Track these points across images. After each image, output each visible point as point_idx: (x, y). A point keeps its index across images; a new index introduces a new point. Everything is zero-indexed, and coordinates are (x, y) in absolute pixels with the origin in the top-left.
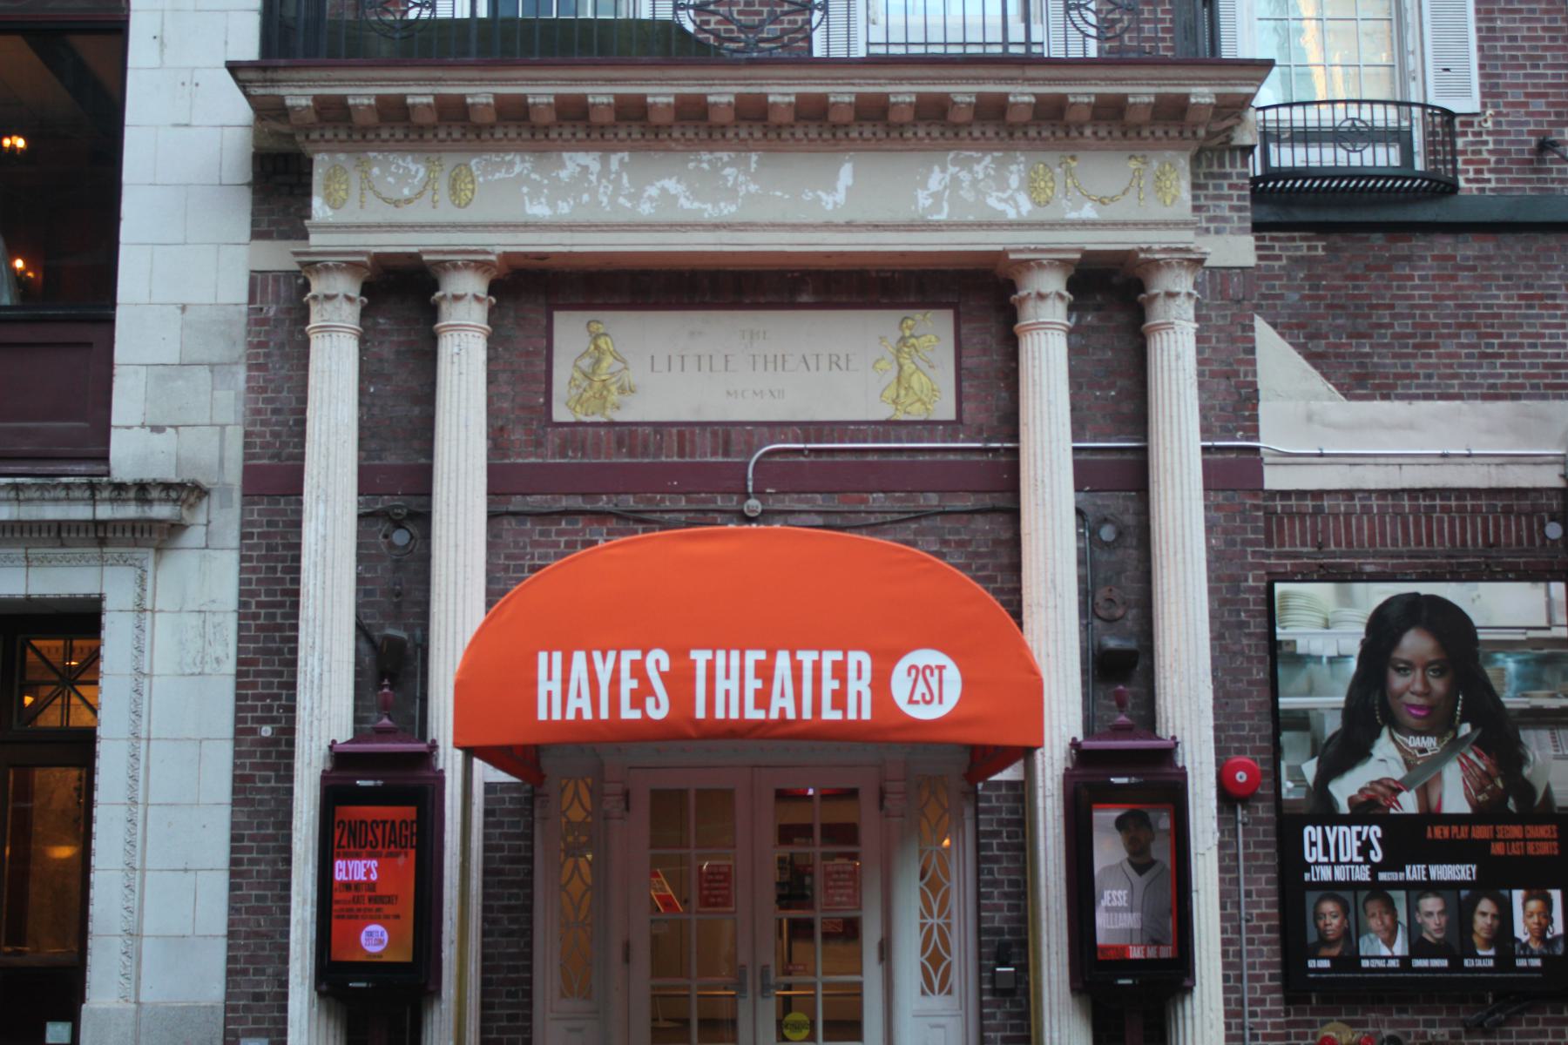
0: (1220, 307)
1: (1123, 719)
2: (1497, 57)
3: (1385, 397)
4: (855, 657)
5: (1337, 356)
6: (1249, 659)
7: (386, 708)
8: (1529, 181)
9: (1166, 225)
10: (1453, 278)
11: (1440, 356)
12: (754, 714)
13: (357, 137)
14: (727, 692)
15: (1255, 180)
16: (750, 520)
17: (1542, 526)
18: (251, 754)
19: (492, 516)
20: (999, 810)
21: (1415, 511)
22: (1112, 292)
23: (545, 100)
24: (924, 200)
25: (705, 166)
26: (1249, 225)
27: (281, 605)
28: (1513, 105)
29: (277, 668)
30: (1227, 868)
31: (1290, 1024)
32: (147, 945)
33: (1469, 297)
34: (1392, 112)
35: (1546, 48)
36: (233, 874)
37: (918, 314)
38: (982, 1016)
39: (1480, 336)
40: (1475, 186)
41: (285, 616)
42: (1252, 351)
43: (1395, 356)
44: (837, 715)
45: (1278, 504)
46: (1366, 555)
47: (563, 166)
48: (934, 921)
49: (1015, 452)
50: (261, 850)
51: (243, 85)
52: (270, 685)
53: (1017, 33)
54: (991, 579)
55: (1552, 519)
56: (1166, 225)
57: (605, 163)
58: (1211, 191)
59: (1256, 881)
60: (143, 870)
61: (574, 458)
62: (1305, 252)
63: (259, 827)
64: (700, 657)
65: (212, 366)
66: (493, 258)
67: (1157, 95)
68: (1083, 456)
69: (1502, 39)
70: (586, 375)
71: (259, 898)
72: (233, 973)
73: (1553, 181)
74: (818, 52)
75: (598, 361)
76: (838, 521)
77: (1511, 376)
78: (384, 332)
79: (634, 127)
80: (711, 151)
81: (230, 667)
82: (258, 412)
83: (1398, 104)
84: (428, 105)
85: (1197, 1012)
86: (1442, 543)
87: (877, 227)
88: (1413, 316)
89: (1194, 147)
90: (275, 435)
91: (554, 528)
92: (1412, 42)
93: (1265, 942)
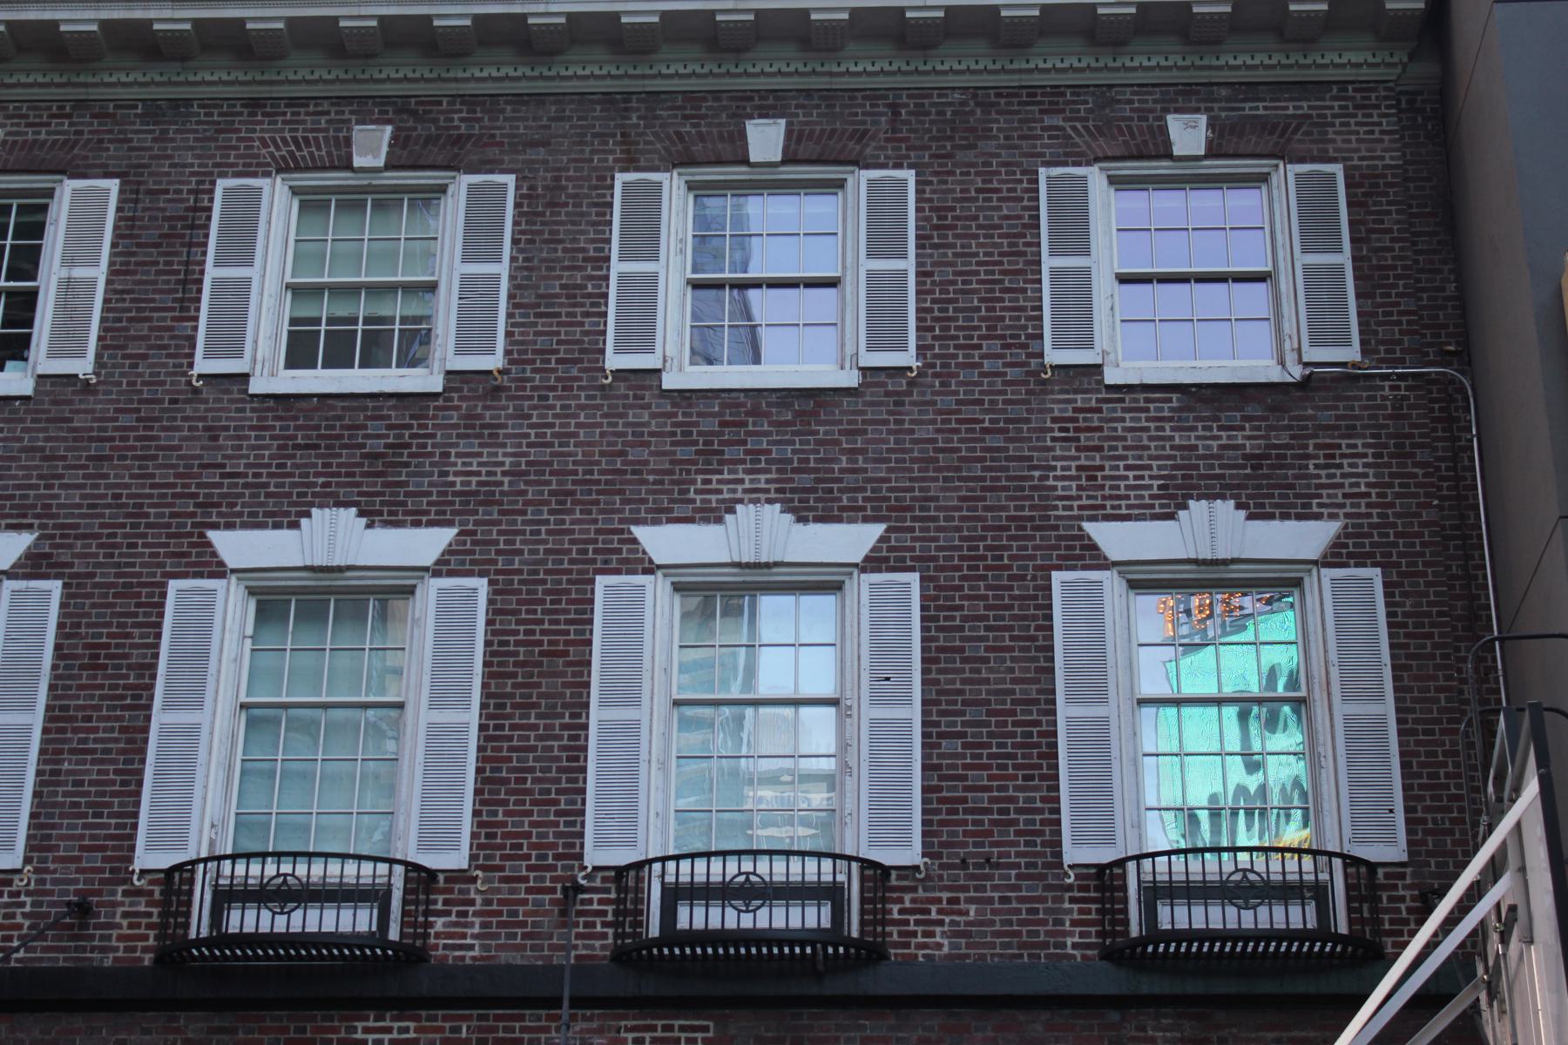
2: (55, 805)
28: (63, 860)
35: (114, 794)
69: (66, 783)
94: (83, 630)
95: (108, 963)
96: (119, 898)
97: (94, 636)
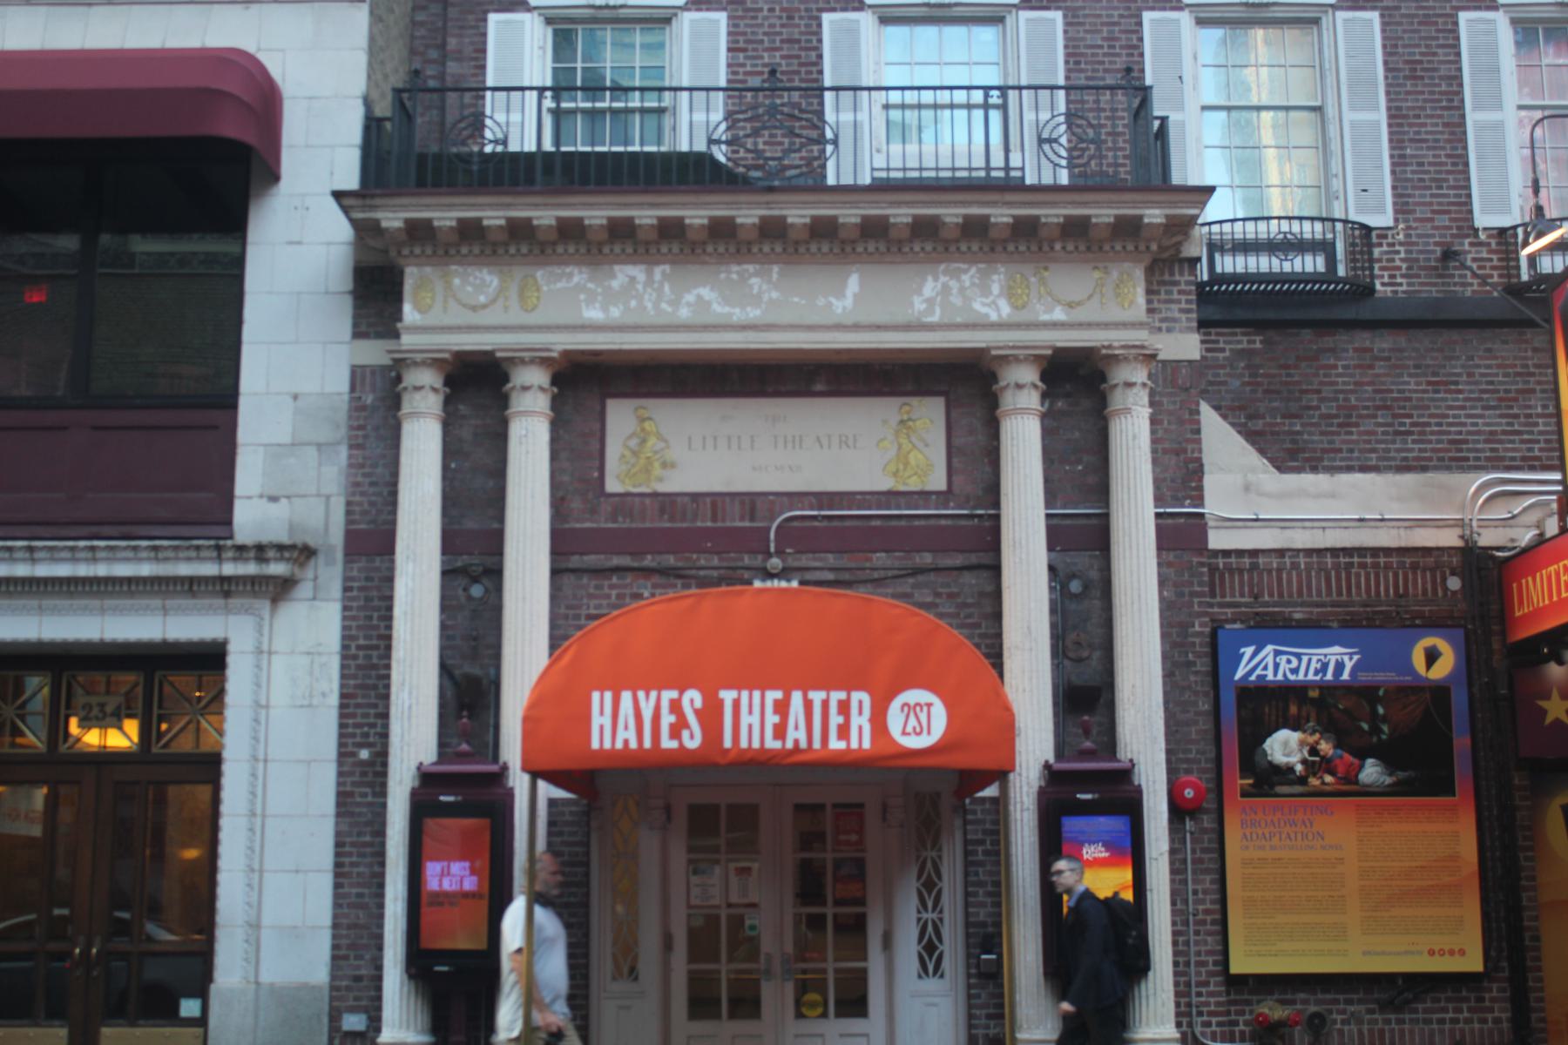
0: (1170, 395)
1: (1088, 744)
2: (1407, 180)
3: (1314, 470)
4: (861, 698)
5: (1273, 433)
6: (1196, 693)
7: (466, 736)
8: (1435, 285)
9: (1124, 325)
10: (1371, 367)
11: (1360, 433)
12: (772, 744)
13: (441, 252)
14: (750, 726)
15: (1201, 286)
16: (771, 576)
17: (1444, 580)
18: (351, 774)
19: (555, 572)
20: (983, 822)
21: (1337, 566)
22: (1077, 380)
23: (598, 222)
24: (919, 305)
25: (735, 276)
26: (1195, 324)
27: (377, 647)
29: (373, 701)
30: (1177, 869)
31: (1230, 1003)
32: (265, 935)
33: (1383, 383)
34: (1318, 226)
35: (1448, 172)
36: (337, 875)
37: (915, 401)
38: (969, 997)
39: (1395, 416)
40: (1389, 289)
41: (380, 657)
42: (1198, 431)
43: (1323, 433)
44: (842, 745)
45: (1221, 562)
46: (1295, 605)
47: (614, 276)
48: (930, 916)
49: (997, 517)
50: (360, 855)
51: (346, 210)
52: (366, 715)
53: (997, 160)
54: (977, 625)
55: (1453, 574)
56: (1124, 325)
57: (650, 274)
58: (1163, 296)
59: (1203, 881)
60: (261, 871)
61: (623, 524)
62: (1245, 345)
63: (359, 834)
64: (728, 696)
65: (319, 446)
66: (555, 355)
67: (1116, 217)
68: (1055, 521)
70: (635, 453)
71: (360, 895)
72: (336, 958)
73: (1455, 284)
74: (831, 180)
75: (644, 441)
76: (846, 576)
77: (1420, 450)
78: (463, 417)
79: (672, 243)
80: (739, 263)
81: (334, 699)
82: (357, 484)
83: (1323, 220)
84: (500, 227)
85: (1151, 991)
86: (1359, 594)
87: (879, 327)
88: (1337, 400)
89: (1147, 259)
90: (372, 504)
91: (606, 583)
92: (1335, 167)
93: (1209, 933)
94: (1400, 50)
95: (1468, 294)
96: (1467, 247)
97: (1410, 54)
